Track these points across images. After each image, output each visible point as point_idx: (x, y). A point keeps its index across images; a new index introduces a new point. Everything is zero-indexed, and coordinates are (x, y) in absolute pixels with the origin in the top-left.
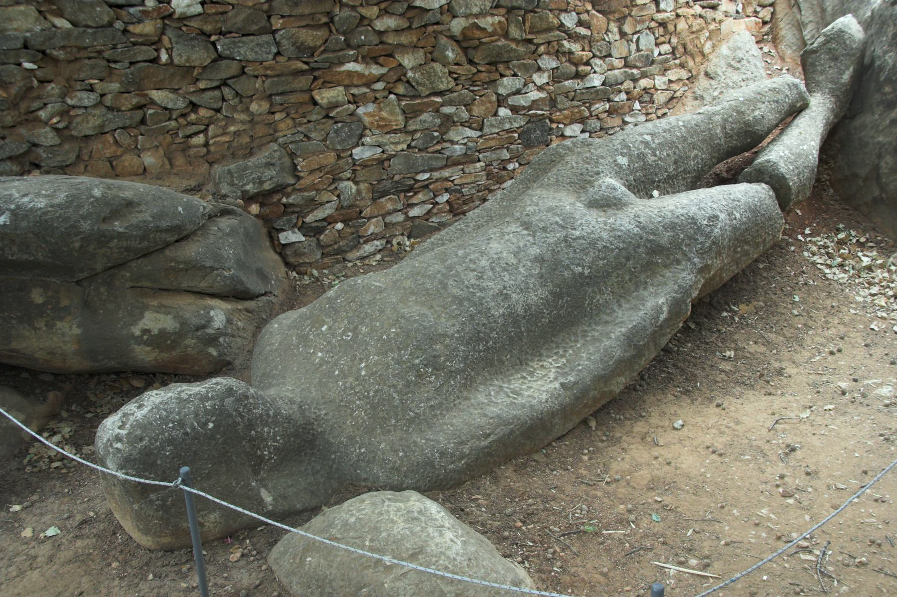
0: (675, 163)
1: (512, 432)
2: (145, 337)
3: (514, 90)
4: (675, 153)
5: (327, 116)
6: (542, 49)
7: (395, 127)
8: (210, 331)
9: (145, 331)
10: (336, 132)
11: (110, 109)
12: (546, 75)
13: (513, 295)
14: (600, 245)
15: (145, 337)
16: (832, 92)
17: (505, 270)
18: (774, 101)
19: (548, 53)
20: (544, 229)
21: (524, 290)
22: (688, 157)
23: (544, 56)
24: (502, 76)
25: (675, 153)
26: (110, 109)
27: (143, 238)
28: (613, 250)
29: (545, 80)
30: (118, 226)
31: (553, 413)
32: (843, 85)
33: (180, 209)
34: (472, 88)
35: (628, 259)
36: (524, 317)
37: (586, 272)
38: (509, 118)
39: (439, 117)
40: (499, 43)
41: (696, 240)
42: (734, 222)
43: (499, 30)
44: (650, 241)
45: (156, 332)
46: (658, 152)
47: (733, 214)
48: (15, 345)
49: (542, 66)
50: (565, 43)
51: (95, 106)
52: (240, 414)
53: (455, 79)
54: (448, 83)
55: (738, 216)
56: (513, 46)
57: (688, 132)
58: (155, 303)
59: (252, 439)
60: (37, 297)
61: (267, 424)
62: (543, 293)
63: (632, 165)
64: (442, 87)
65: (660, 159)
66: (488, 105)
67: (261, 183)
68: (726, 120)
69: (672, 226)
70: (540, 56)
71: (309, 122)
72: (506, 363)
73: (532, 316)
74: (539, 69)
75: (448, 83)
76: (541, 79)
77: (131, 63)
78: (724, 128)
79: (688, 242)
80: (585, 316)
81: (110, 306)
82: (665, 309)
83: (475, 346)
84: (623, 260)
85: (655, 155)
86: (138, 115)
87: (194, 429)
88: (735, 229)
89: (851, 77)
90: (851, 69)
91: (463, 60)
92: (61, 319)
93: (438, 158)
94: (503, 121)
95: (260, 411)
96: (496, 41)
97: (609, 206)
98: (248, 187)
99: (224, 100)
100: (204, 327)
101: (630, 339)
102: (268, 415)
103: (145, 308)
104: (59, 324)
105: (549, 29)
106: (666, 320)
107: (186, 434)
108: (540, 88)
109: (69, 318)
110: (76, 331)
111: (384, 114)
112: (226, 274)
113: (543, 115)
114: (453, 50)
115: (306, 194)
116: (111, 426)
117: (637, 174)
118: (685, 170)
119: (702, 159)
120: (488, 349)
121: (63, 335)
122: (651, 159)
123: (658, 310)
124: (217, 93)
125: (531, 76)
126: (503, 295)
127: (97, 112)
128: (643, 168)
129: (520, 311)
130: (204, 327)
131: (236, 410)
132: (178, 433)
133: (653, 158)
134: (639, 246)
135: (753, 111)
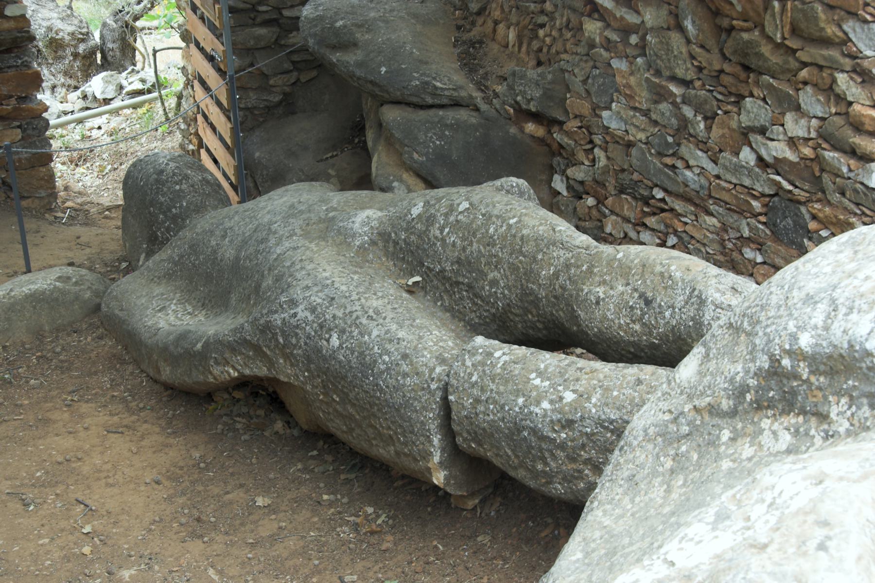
0: (459, 262)
3: (757, 124)
4: (464, 249)
5: (588, 55)
6: (804, 73)
7: (637, 105)
10: (594, 77)
12: (803, 122)
13: (227, 239)
18: (642, 296)
19: (815, 85)
22: (483, 274)
23: (809, 89)
24: (752, 95)
25: (464, 249)
29: (801, 133)
33: (383, 69)
34: (715, 94)
38: (750, 171)
39: (676, 116)
40: (745, 36)
42: (325, 343)
43: (751, 14)
46: (447, 230)
47: (330, 330)
49: (802, 105)
50: (842, 78)
53: (700, 69)
54: (687, 69)
55: (335, 341)
56: (766, 49)
57: (504, 238)
59: (150, 212)
61: (164, 213)
64: (680, 72)
65: (443, 240)
66: (726, 131)
67: (529, 101)
68: (568, 266)
70: (805, 83)
71: (577, 54)
74: (798, 108)
75: (687, 69)
76: (795, 127)
78: (556, 275)
83: (191, 254)
85: (442, 233)
91: (711, 43)
93: (668, 176)
94: (738, 169)
95: (163, 199)
96: (747, 30)
98: (519, 98)
105: (826, 42)
108: (792, 142)
111: (633, 80)
112: (416, 156)
113: (790, 192)
114: (693, 22)
115: (566, 140)
117: (413, 238)
118: (470, 287)
120: (193, 264)
122: (435, 231)
125: (783, 114)
131: (152, 185)
133: (438, 233)
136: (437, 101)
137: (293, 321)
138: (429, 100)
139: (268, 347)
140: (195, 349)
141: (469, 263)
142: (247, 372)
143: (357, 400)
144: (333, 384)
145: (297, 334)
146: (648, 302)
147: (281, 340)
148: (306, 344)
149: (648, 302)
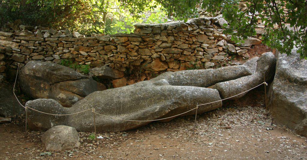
1: (103, 124)
2: (59, 99)
8: (73, 101)
9: (59, 97)
11: (71, 54)
14: (148, 91)
15: (59, 99)
16: (261, 72)
17: (123, 92)
18: (234, 70)
20: (138, 86)
21: (124, 97)
26: (71, 54)
27: (60, 76)
28: (151, 93)
30: (55, 72)
31: (117, 124)
32: (265, 70)
35: (154, 96)
36: (122, 103)
37: (142, 97)
41: (175, 95)
44: (162, 93)
45: (61, 98)
47: (194, 92)
48: (37, 95)
51: (68, 52)
52: (51, 106)
55: (196, 93)
58: (63, 92)
60: (42, 86)
61: (57, 110)
62: (129, 99)
63: (174, 78)
65: (185, 78)
67: (99, 74)
69: (170, 91)
72: (114, 112)
73: (124, 104)
77: (77, 45)
79: (173, 95)
80: (139, 107)
81: (55, 91)
82: (158, 109)
84: (153, 96)
86: (77, 56)
87: (41, 105)
88: (194, 96)
89: (269, 69)
90: (268, 66)
92: (45, 91)
97: (158, 85)
98: (95, 74)
99: (96, 55)
100: (71, 99)
101: (144, 114)
102: (58, 109)
103: (61, 93)
104: (45, 92)
106: (158, 111)
107: (39, 106)
109: (47, 91)
110: (48, 95)
116: (29, 102)
118: (194, 83)
119: (203, 81)
121: (45, 95)
122: (181, 77)
123: (156, 109)
124: (95, 53)
126: (118, 97)
127: (69, 54)
128: (178, 79)
129: (122, 102)
130: (71, 99)
132: (38, 105)
134: (158, 94)
135: (225, 72)
136: (79, 78)
137: (187, 93)
138: (78, 78)
139: (180, 101)
140: (155, 111)
141: (194, 79)
142: (173, 109)
143: (203, 101)
144: (197, 101)
145: (188, 95)
146: (235, 71)
147: (185, 98)
148: (190, 96)
149: (235, 71)
